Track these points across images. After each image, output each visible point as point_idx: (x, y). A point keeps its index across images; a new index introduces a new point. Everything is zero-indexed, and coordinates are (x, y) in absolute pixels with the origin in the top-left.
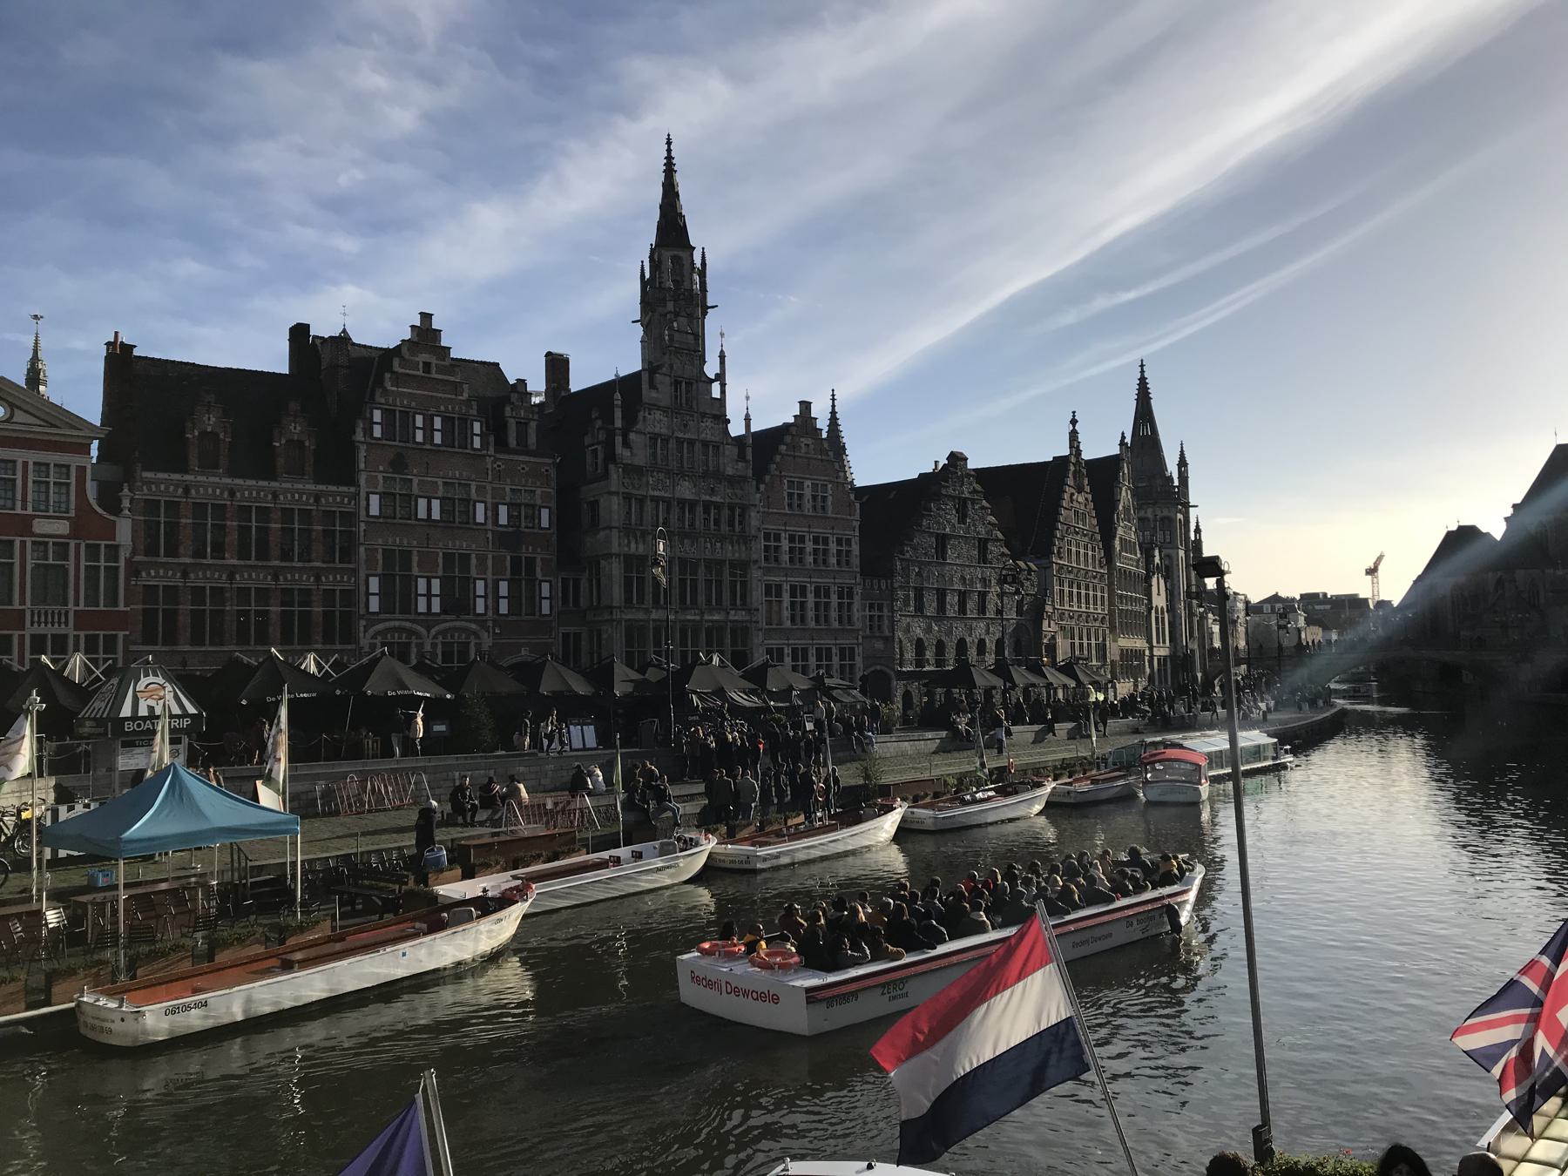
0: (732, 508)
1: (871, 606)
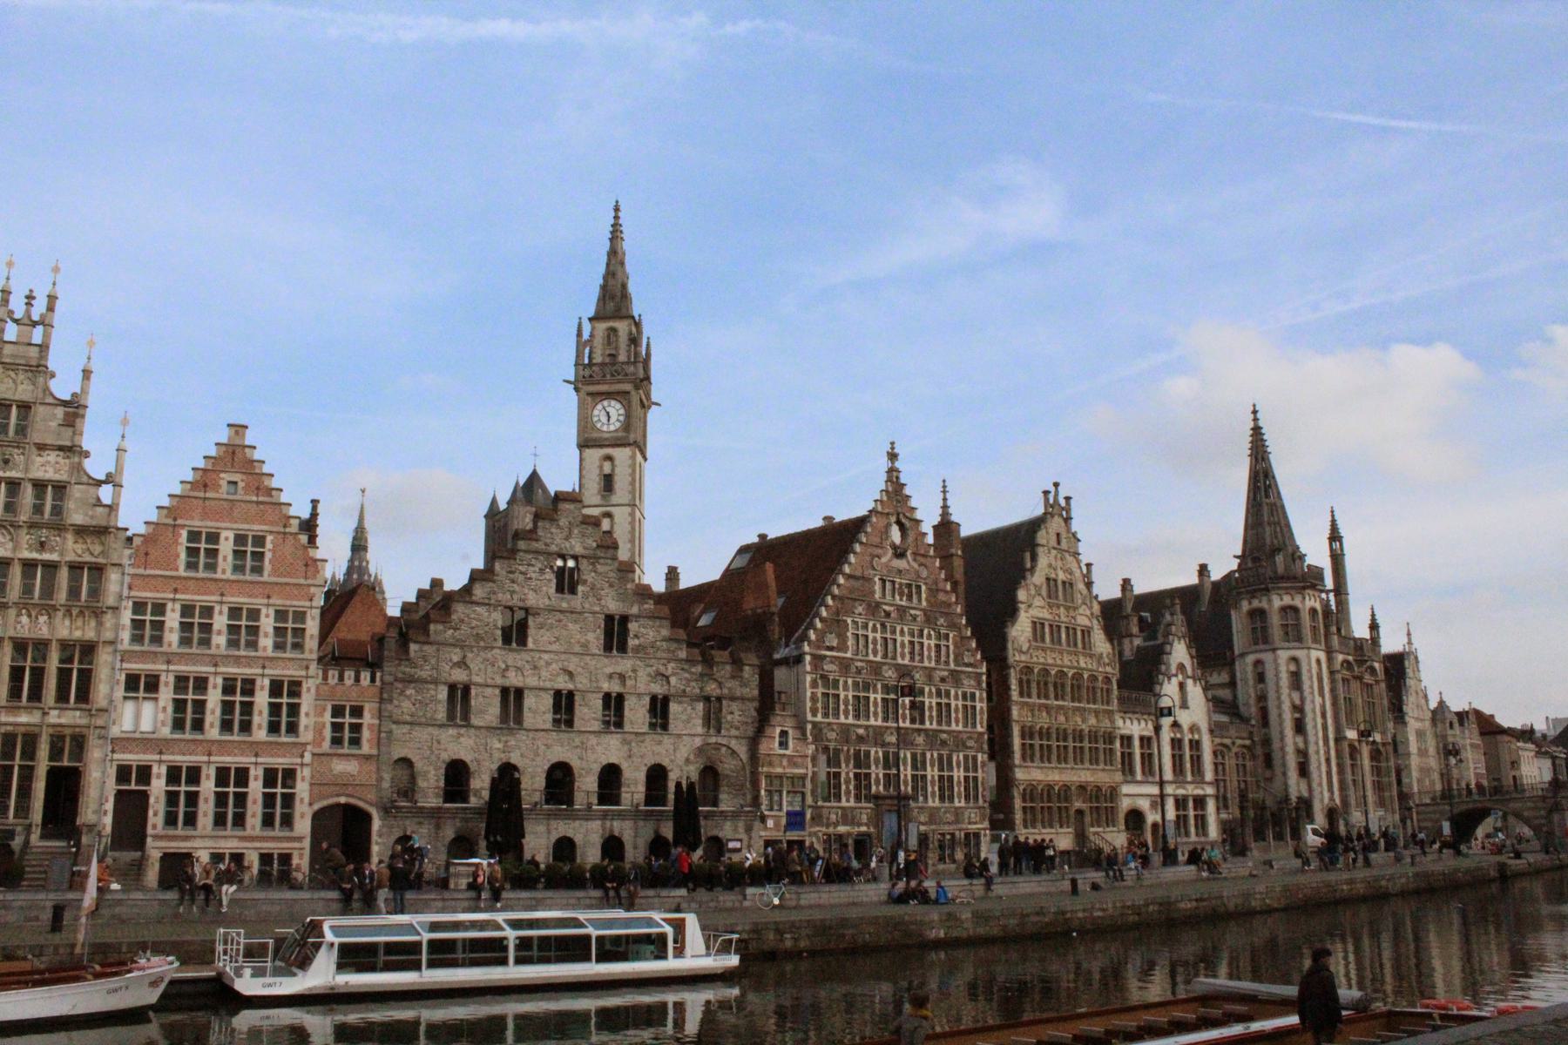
0: (75, 568)
1: (338, 711)
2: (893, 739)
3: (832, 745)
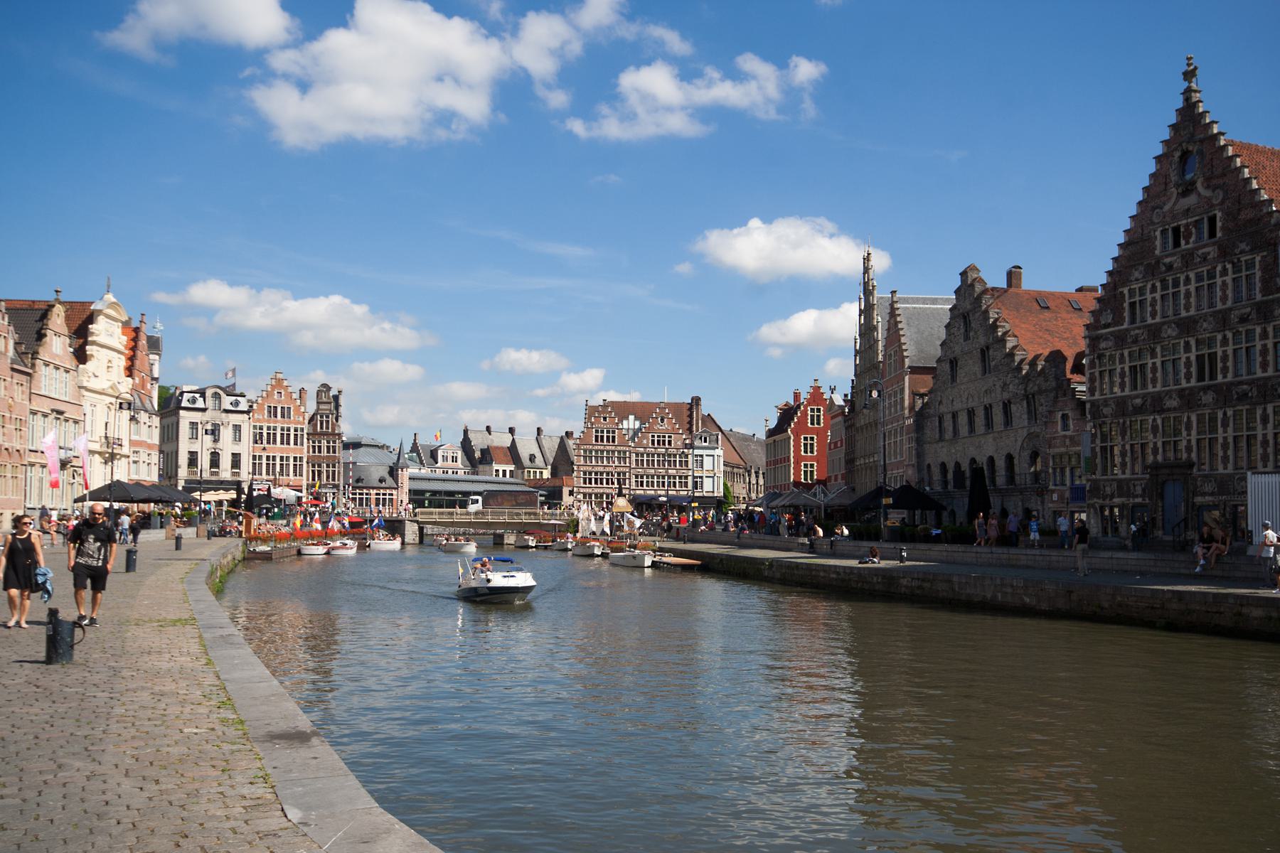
2: (1173, 403)
3: (1108, 420)
